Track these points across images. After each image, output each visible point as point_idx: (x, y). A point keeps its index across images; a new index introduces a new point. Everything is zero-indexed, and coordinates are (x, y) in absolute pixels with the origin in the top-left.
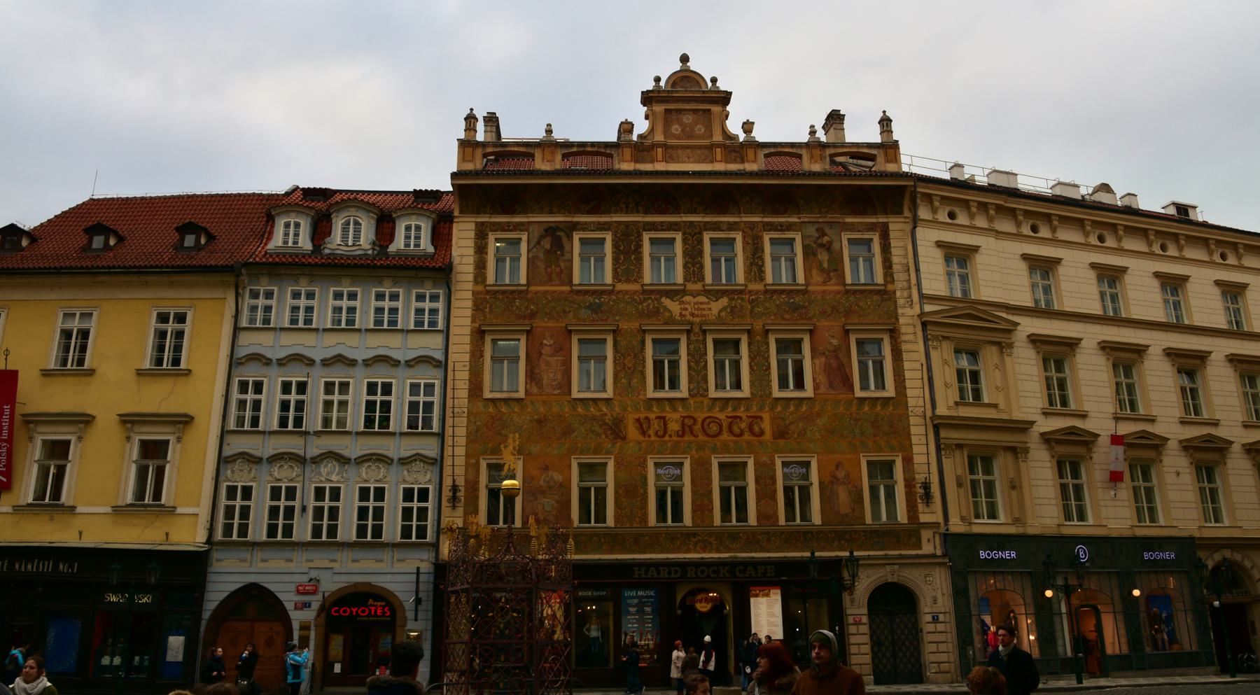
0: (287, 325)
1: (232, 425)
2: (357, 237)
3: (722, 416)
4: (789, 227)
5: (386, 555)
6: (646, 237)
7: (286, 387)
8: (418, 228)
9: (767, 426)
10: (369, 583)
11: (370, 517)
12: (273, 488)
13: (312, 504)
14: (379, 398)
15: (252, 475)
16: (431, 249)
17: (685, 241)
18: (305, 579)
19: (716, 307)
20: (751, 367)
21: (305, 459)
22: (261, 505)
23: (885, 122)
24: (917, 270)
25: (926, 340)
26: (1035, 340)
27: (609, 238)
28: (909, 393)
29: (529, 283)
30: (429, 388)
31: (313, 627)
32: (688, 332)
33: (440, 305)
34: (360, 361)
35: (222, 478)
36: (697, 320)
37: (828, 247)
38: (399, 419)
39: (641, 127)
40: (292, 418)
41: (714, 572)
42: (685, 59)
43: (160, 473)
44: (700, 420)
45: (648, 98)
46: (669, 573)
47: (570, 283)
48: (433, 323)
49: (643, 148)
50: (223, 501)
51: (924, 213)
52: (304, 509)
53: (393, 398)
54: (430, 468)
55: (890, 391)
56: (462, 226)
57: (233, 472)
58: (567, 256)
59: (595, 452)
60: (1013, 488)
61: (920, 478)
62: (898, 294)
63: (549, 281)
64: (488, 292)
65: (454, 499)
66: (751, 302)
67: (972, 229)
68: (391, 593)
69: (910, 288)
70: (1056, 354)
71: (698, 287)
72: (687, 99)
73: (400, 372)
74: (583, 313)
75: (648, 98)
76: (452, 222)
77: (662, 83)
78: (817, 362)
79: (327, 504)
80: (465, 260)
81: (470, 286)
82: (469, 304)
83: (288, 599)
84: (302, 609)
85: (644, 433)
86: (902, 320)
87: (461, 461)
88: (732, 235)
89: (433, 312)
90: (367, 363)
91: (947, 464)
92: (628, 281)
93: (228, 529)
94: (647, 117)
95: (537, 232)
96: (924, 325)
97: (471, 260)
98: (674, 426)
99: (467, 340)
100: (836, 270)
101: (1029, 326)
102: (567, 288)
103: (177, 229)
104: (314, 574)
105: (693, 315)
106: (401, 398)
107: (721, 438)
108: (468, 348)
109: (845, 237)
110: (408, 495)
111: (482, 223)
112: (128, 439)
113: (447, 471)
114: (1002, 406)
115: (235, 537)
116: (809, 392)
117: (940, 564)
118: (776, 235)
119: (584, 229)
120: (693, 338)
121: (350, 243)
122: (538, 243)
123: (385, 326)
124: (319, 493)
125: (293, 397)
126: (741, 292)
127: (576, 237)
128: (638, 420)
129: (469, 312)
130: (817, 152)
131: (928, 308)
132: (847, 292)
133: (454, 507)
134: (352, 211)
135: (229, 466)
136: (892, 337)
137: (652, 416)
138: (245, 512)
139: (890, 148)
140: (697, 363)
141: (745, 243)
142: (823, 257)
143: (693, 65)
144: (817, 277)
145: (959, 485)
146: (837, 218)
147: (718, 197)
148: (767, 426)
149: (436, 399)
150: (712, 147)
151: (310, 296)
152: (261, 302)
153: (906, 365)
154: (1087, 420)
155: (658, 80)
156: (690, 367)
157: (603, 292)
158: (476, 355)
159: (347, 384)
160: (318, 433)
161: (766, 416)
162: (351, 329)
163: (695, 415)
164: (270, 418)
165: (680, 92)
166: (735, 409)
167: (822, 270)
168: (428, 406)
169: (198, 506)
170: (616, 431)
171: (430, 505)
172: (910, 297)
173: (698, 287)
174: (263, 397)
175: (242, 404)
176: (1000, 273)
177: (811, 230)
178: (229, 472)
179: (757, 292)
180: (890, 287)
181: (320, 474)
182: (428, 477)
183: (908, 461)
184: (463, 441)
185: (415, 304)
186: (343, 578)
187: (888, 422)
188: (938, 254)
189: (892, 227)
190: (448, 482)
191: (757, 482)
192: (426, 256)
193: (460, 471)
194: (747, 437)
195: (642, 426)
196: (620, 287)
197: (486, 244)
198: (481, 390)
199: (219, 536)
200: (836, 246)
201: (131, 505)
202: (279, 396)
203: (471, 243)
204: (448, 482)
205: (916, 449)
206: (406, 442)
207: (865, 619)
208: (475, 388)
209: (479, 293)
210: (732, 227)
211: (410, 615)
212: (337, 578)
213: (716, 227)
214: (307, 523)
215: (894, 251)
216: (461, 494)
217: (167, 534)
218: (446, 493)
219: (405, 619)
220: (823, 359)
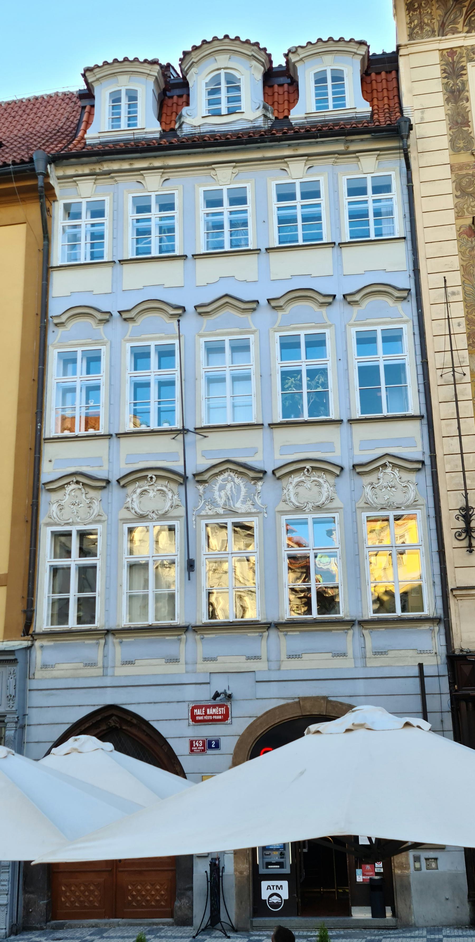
5: (350, 640)
7: (140, 356)
10: (325, 698)
15: (96, 507)
16: (364, 108)
18: (204, 695)
21: (185, 478)
30: (393, 338)
34: (263, 302)
35: (43, 519)
38: (344, 398)
54: (412, 477)
56: (415, 60)
57: (61, 508)
80: (429, 115)
81: (445, 157)
82: (449, 187)
97: (441, 113)
99: (453, 248)
104: (220, 685)
106: (343, 359)
111: (452, 51)
123: (301, 242)
129: (449, 202)
134: (222, 60)
135: (54, 497)
138: (87, 577)
149: (408, 355)
168: (395, 373)
174: (102, 378)
178: (54, 508)
181: (213, 503)
182: (412, 495)
186: (273, 690)
192: (359, 120)
197: (464, 84)
203: (437, 86)
204: (451, 502)
206: (362, 432)
209: (461, 167)
212: (263, 690)
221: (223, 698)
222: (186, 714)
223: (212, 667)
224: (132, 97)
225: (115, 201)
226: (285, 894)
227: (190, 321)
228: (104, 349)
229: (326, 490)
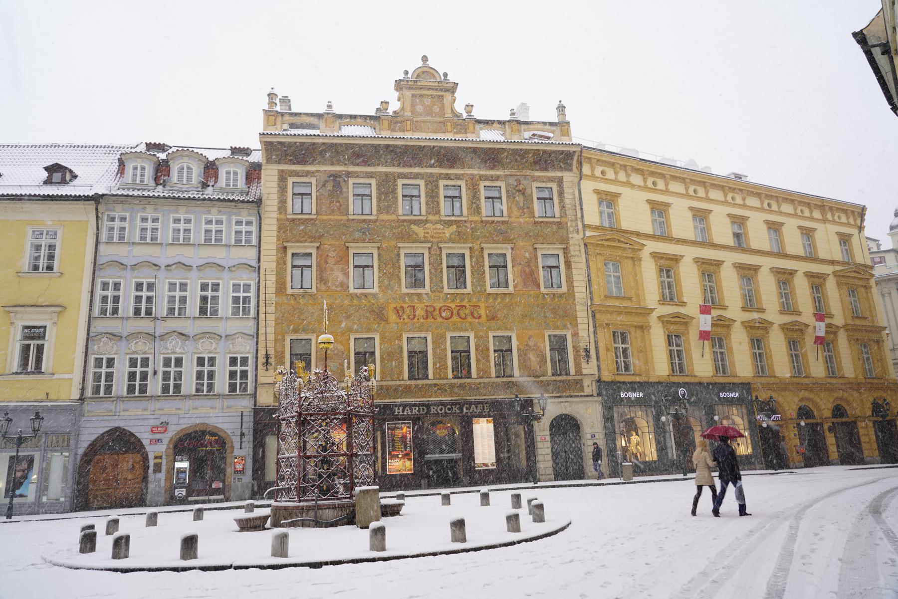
0: (138, 240)
1: (96, 312)
2: (189, 178)
3: (453, 306)
4: (498, 178)
6: (400, 182)
7: (139, 287)
8: (235, 173)
9: (482, 312)
11: (205, 378)
12: (131, 359)
13: (161, 369)
14: (209, 294)
17: (426, 185)
18: (158, 423)
19: (448, 232)
20: (472, 273)
22: (121, 370)
23: (561, 108)
24: (582, 209)
25: (586, 253)
26: (655, 256)
27: (373, 182)
28: (576, 290)
29: (317, 213)
30: (247, 287)
31: (164, 457)
32: (429, 248)
33: (254, 228)
36: (435, 240)
37: (523, 192)
39: (394, 106)
40: (144, 309)
41: (449, 409)
42: (425, 59)
43: (40, 349)
44: (438, 308)
45: (399, 85)
46: (419, 411)
47: (347, 214)
48: (248, 241)
49: (396, 121)
50: (91, 369)
51: (586, 169)
52: (155, 373)
53: (220, 294)
54: (250, 342)
55: (564, 289)
56: (268, 172)
57: (99, 348)
58: (345, 195)
59: (369, 330)
60: (641, 351)
61: (582, 345)
62: (569, 224)
63: (332, 212)
64: (288, 219)
65: (267, 363)
66: (472, 229)
67: (615, 182)
68: (222, 430)
69: (576, 220)
70: (667, 266)
71: (436, 218)
72: (427, 87)
73: (226, 275)
74: (357, 235)
75: (399, 85)
76: (260, 170)
77: (409, 75)
78: (516, 269)
79: (172, 369)
80: (271, 196)
81: (275, 215)
82: (275, 228)
83: (145, 437)
84: (156, 444)
85: (400, 317)
86: (571, 242)
87: (271, 337)
88: (459, 183)
89: (249, 233)
90: (200, 268)
91: (600, 335)
92: (388, 213)
93: (97, 389)
94: (399, 100)
95: (323, 178)
96: (585, 245)
98: (420, 312)
99: (274, 252)
100: (528, 208)
101: (652, 246)
102: (345, 218)
103: (46, 169)
104: (163, 419)
105: (432, 237)
107: (452, 319)
108: (275, 258)
109: (535, 185)
110: (233, 361)
111: (283, 171)
112: (12, 323)
113: (262, 344)
114: (634, 299)
115: (102, 394)
116: (511, 289)
117: (595, 401)
118: (487, 183)
119: (357, 177)
120: (433, 252)
121: (185, 182)
122: (324, 185)
124: (167, 362)
125: (144, 293)
126: (465, 221)
127: (351, 181)
128: (395, 308)
129: (275, 234)
130: (516, 126)
131: (588, 234)
132: (536, 223)
133: (267, 370)
134: (186, 159)
136: (564, 253)
137: (405, 306)
139: (563, 126)
140: (436, 269)
141: (468, 189)
142: (519, 198)
143: (431, 63)
144: (516, 212)
145: (608, 350)
146: (528, 172)
147: (449, 157)
148: (482, 312)
150: (443, 123)
151: (155, 220)
152: (117, 224)
153: (574, 271)
154: (687, 308)
155: (406, 73)
156: (431, 273)
157: (370, 221)
158: (281, 262)
159: (186, 285)
160: (164, 319)
161: (482, 305)
162: (187, 243)
163: (435, 305)
164: (127, 307)
165: (423, 82)
166: (462, 301)
167: (519, 208)
169: (72, 372)
170: (380, 315)
171: (250, 368)
172: (577, 226)
173: (436, 218)
174: (120, 293)
175: (105, 299)
176: (634, 213)
177: (512, 181)
179: (475, 222)
180: (564, 220)
181: (167, 349)
183: (575, 335)
184: (272, 323)
185: (235, 228)
187: (561, 308)
188: (595, 197)
189: (565, 180)
190: (262, 352)
191: (477, 349)
193: (271, 344)
194: (470, 319)
195: (398, 311)
196: (384, 217)
197: (286, 185)
198: (285, 288)
199: (89, 392)
200: (528, 191)
201: (17, 373)
202: (134, 293)
204: (262, 352)
205: (580, 327)
207: (548, 438)
208: (281, 287)
210: (458, 177)
211: (237, 445)
213: (448, 177)
214: (157, 382)
215: (566, 195)
216: (272, 360)
217: (47, 394)
218: (261, 360)
219: (233, 447)
220: (520, 267)
221: (165, 425)
222: (149, 429)
223: (161, 412)
224: (143, 169)
225: (131, 215)
226: (184, 493)
227: (162, 274)
228: (122, 281)
229: (214, 345)
